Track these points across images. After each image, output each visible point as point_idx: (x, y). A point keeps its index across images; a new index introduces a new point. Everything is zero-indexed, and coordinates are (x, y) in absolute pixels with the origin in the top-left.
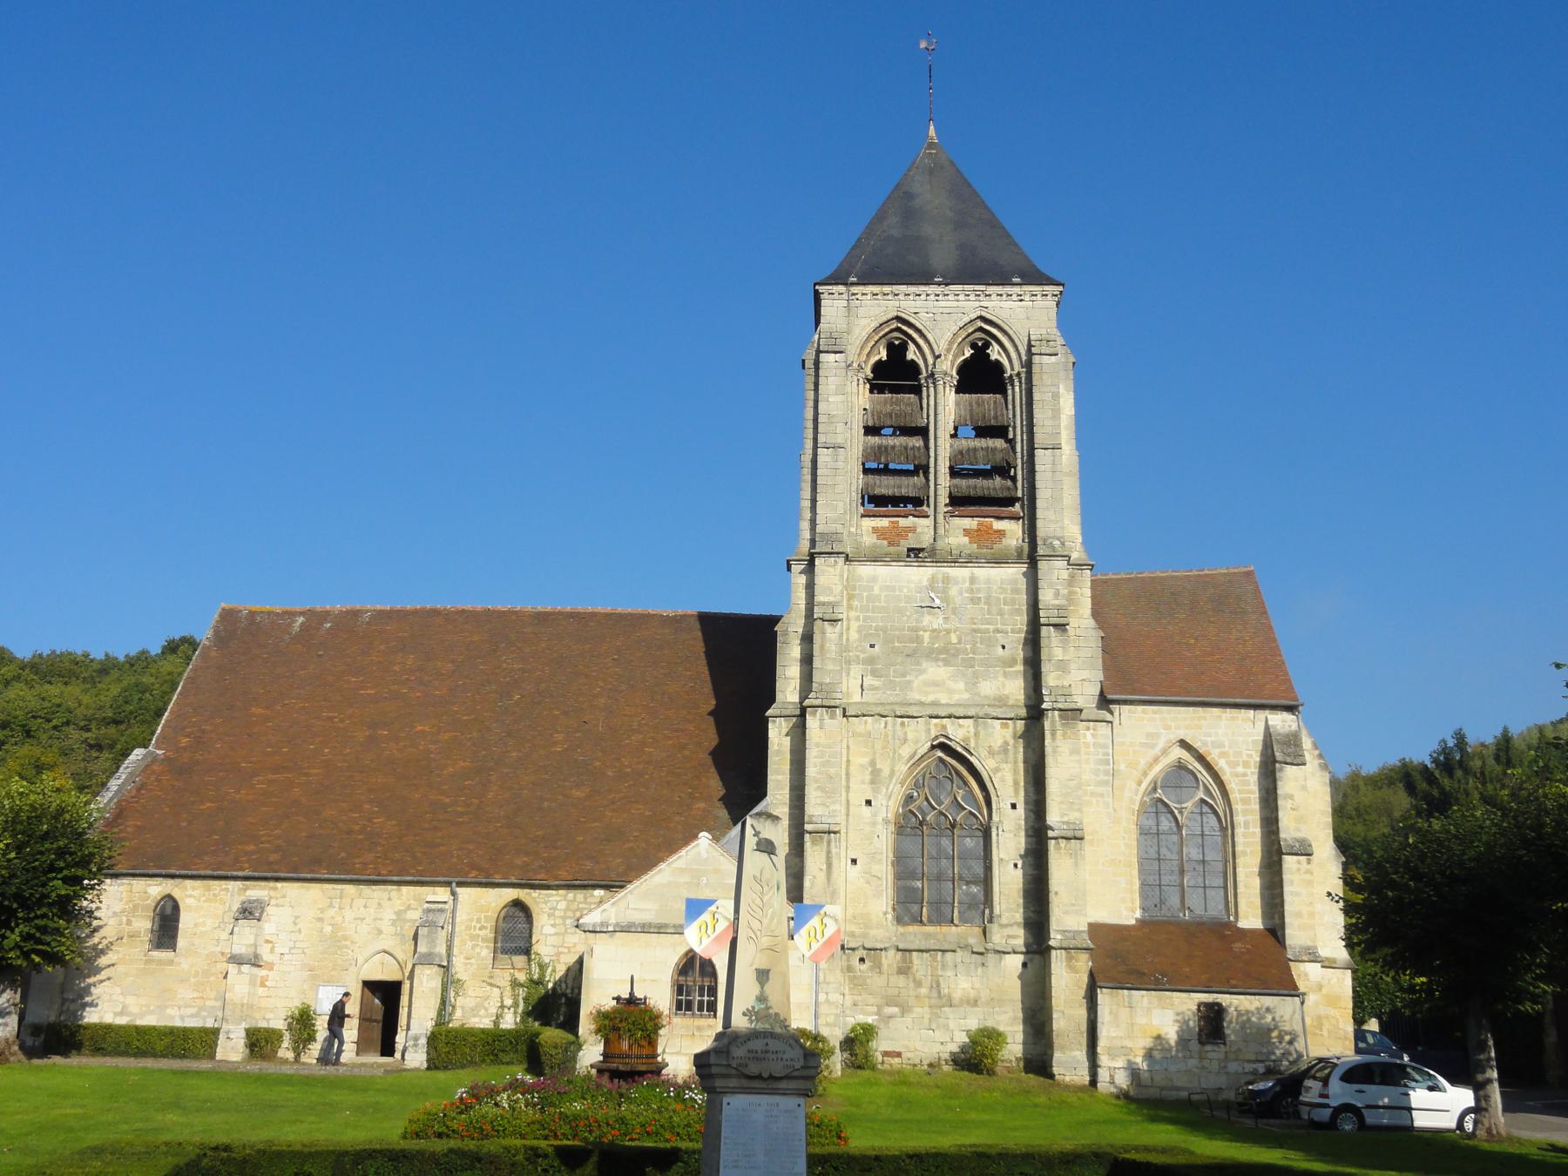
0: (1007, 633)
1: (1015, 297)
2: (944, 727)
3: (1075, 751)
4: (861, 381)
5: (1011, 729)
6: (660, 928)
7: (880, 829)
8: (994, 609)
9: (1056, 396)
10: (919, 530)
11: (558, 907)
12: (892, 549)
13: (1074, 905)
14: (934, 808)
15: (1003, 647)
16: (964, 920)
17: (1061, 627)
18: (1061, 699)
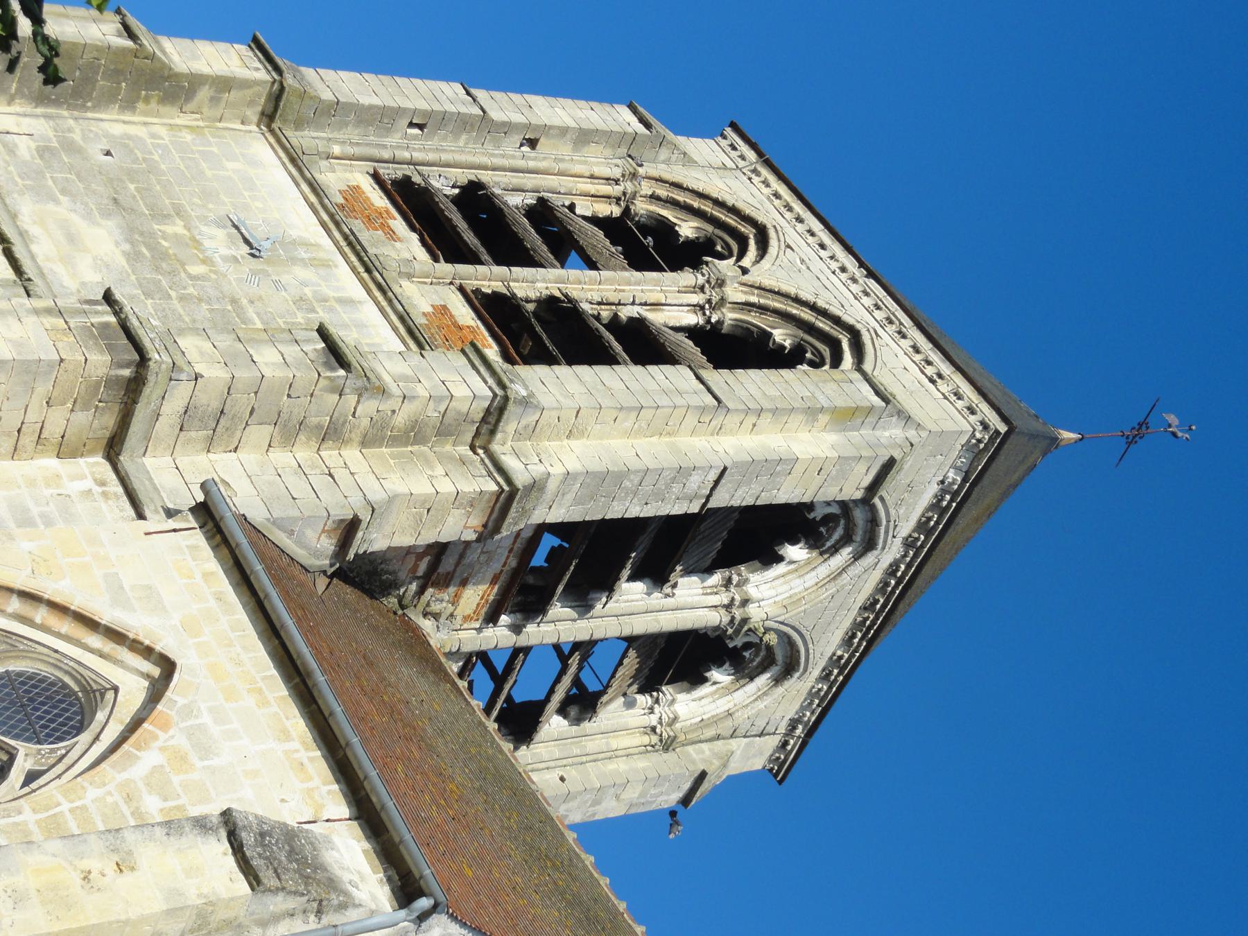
1: (930, 371)
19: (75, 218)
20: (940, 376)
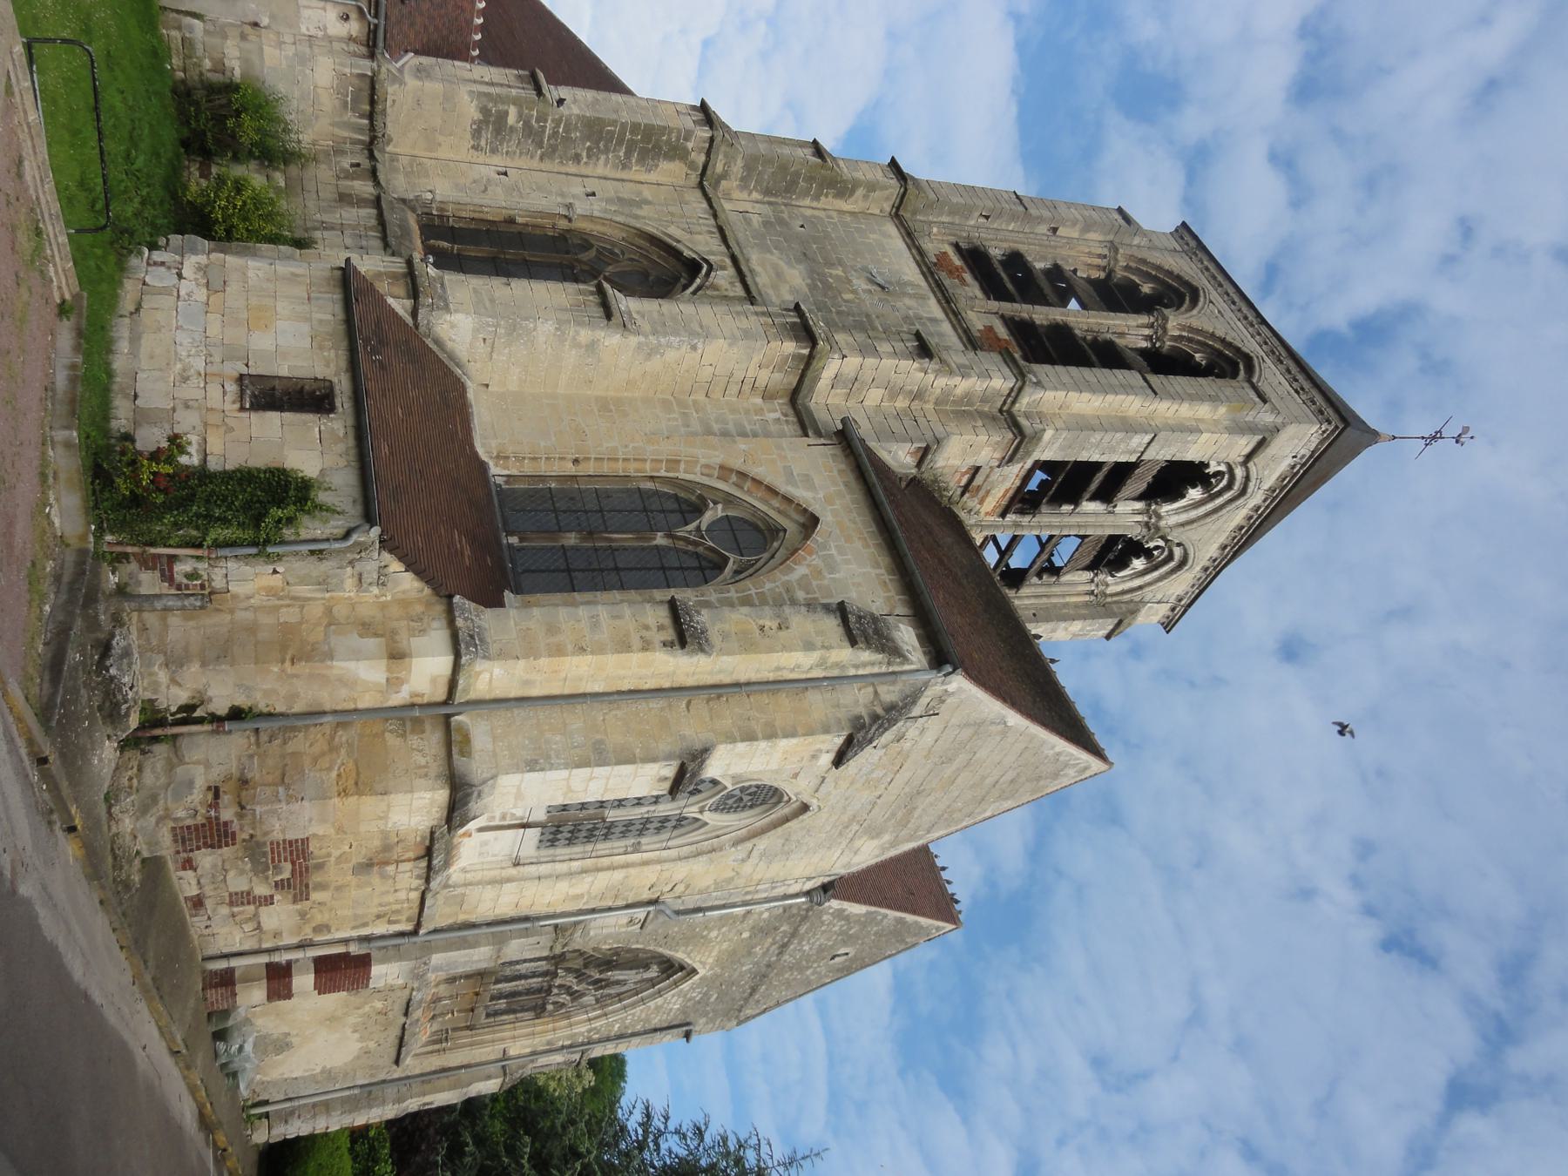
19: (782, 263)
20: (1303, 389)
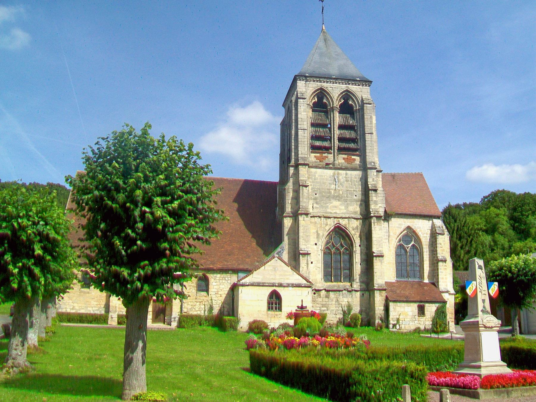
0: (357, 191)
1: (357, 85)
2: (339, 221)
3: (380, 229)
4: (310, 108)
5: (359, 222)
6: (263, 284)
7: (320, 252)
8: (353, 184)
9: (371, 117)
10: (329, 157)
11: (217, 276)
12: (321, 163)
13: (381, 276)
14: (335, 246)
15: (356, 196)
16: (344, 281)
17: (375, 190)
18: (376, 213)
19: (331, 205)
